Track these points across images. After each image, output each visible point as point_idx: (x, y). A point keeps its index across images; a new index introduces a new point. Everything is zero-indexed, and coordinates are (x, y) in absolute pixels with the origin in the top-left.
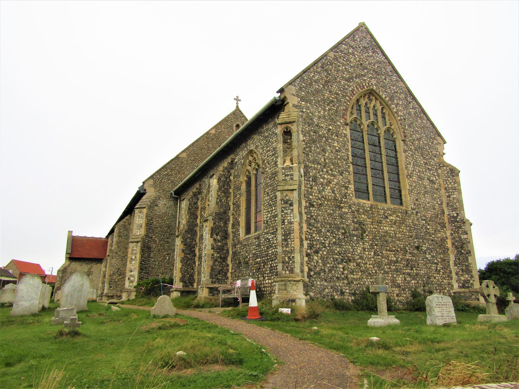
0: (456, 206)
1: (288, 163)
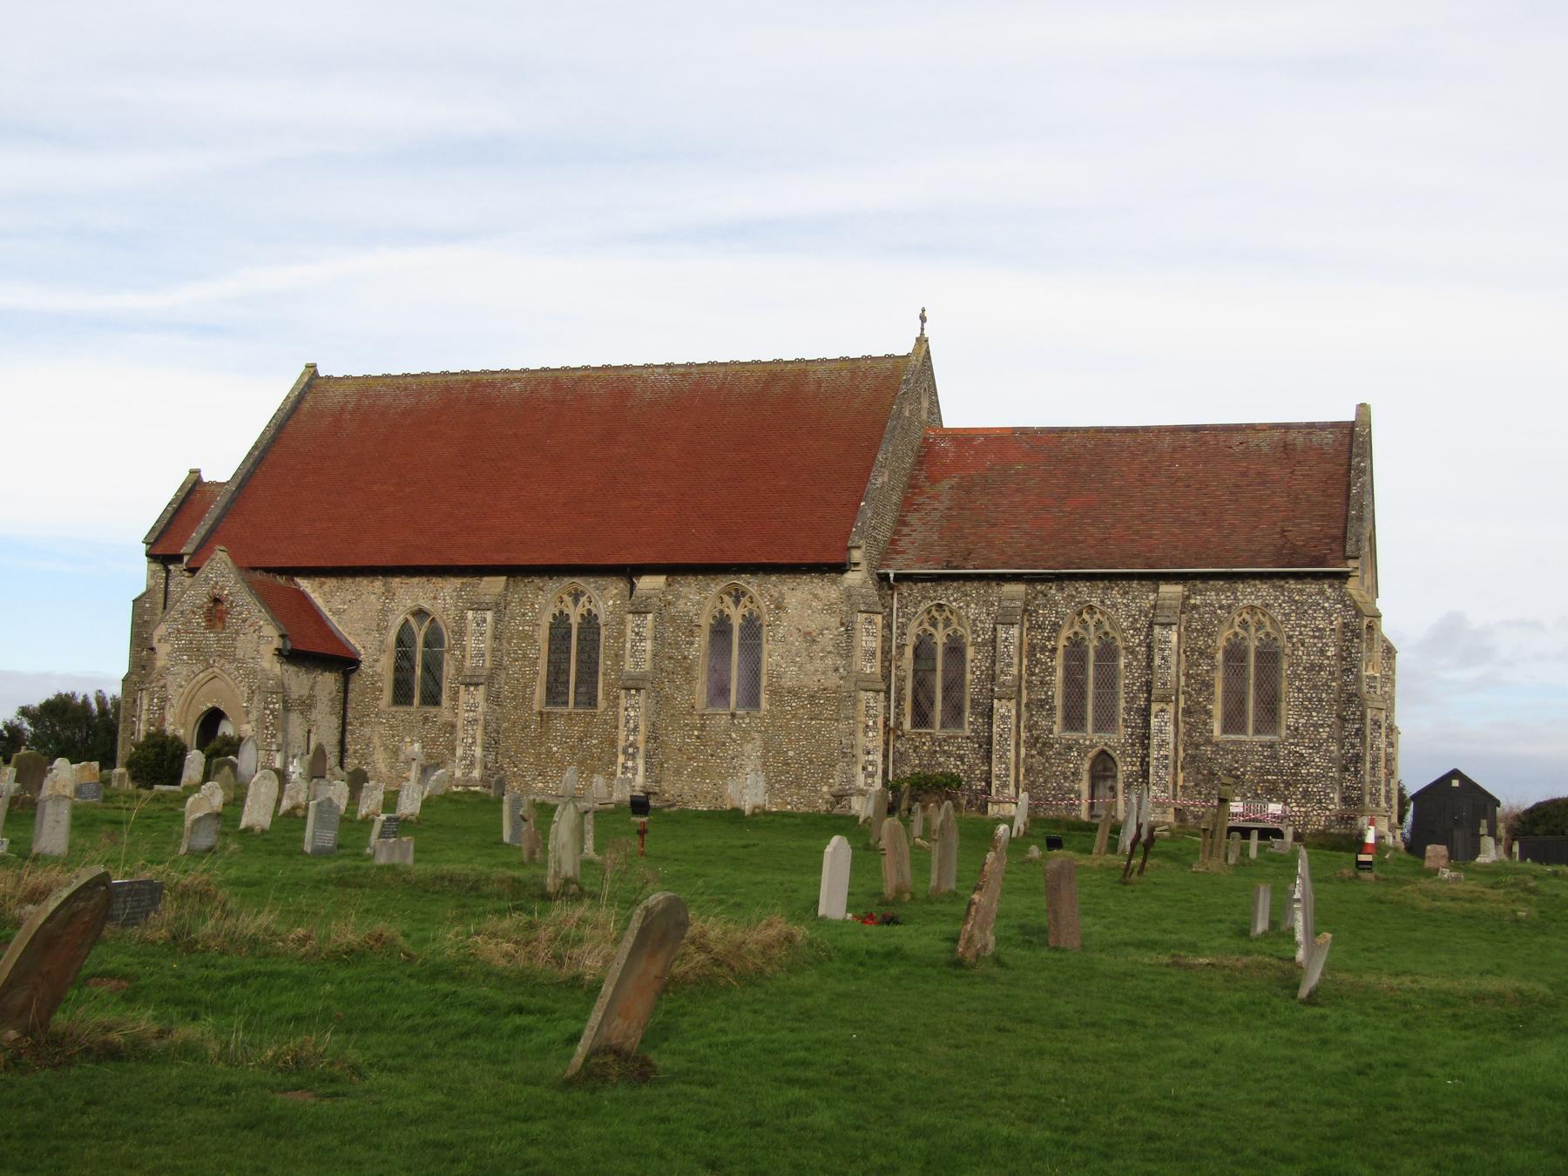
1: (1370, 672)
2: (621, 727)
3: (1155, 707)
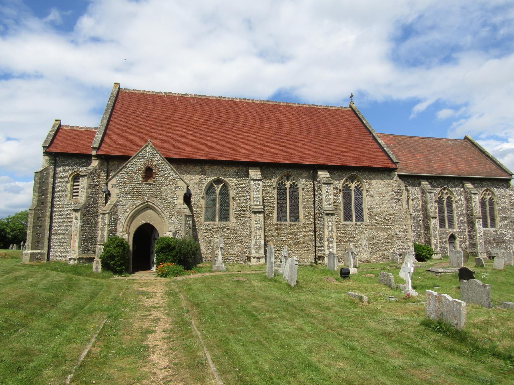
2: (326, 230)
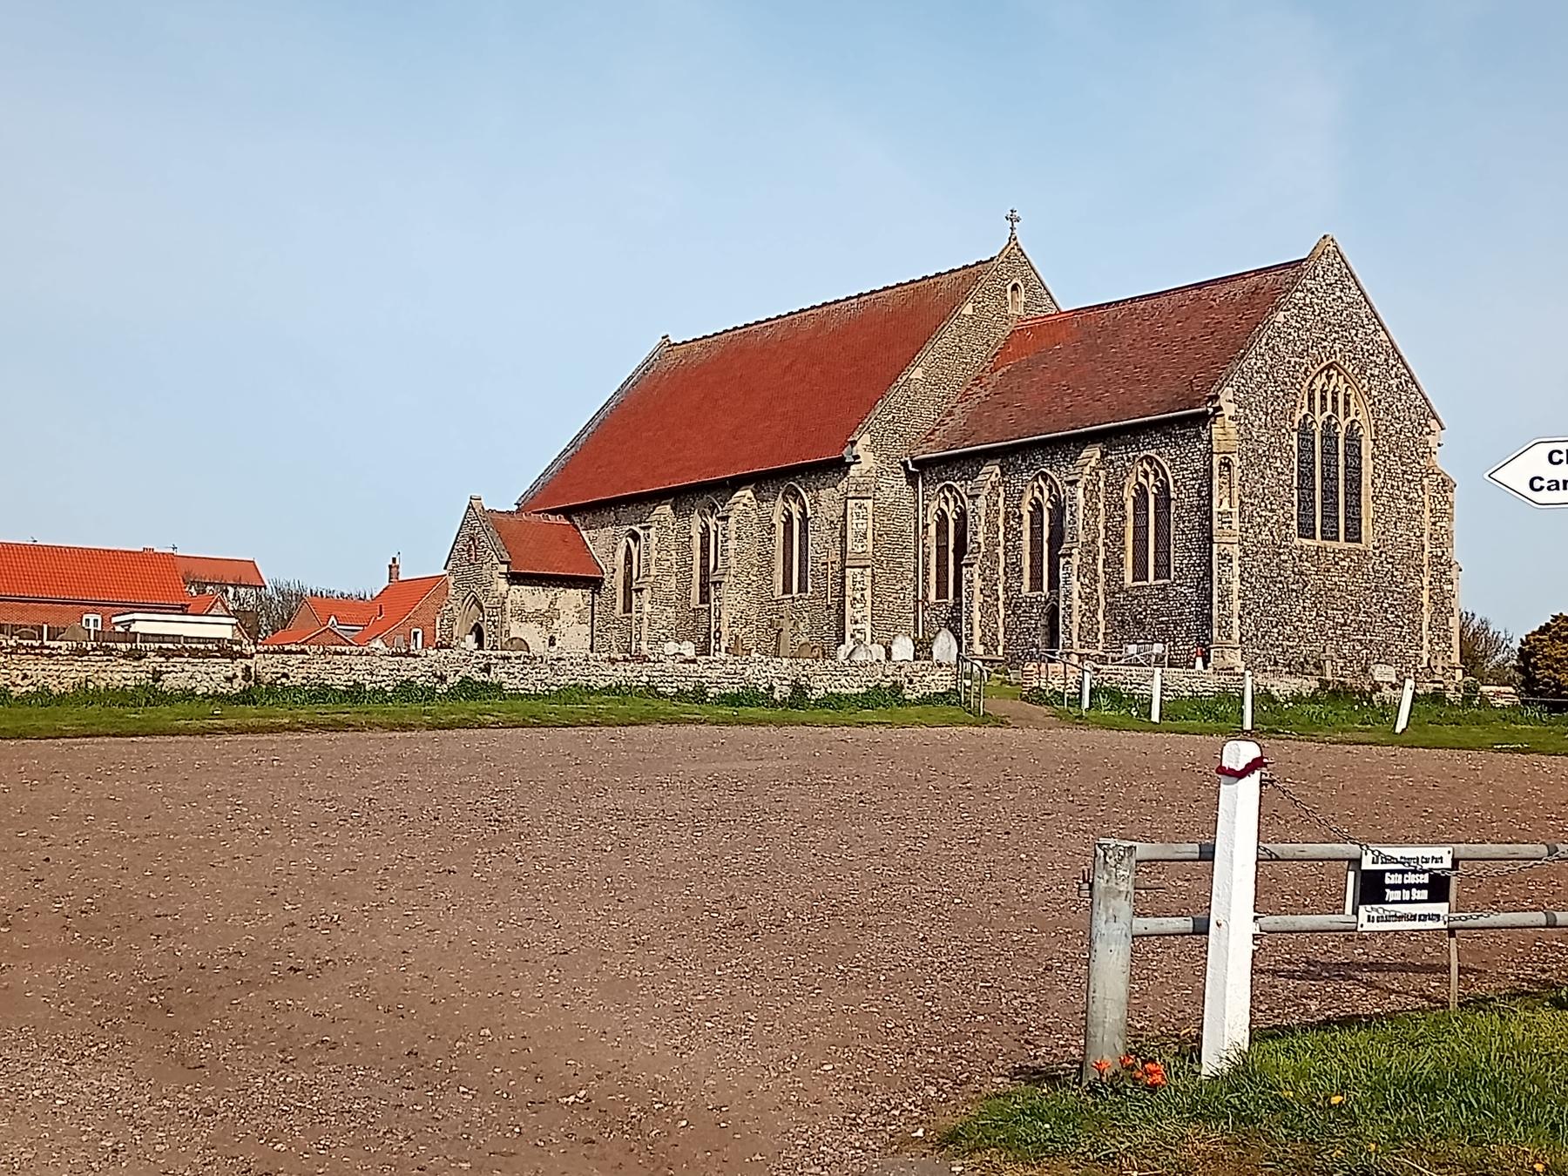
0: (1442, 540)
1: (1225, 506)
3: (1062, 561)
